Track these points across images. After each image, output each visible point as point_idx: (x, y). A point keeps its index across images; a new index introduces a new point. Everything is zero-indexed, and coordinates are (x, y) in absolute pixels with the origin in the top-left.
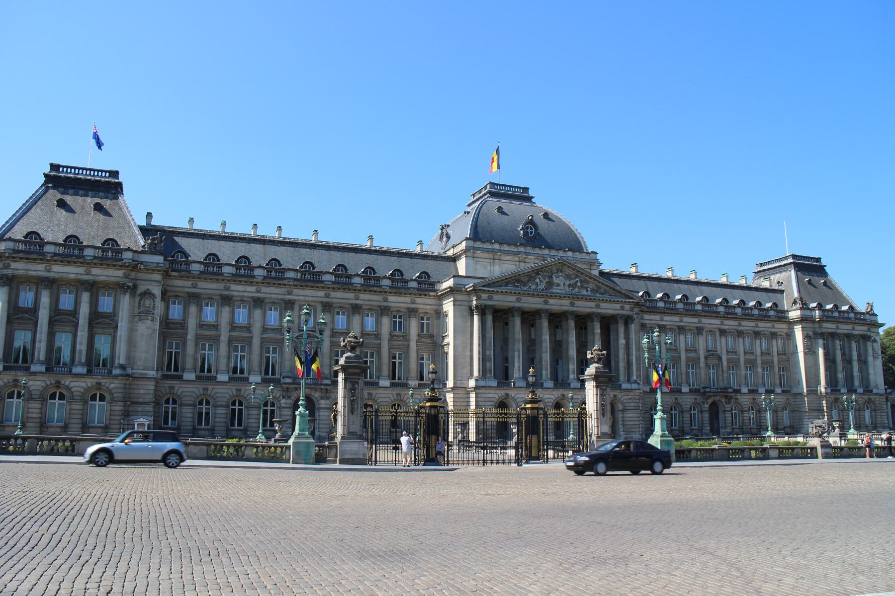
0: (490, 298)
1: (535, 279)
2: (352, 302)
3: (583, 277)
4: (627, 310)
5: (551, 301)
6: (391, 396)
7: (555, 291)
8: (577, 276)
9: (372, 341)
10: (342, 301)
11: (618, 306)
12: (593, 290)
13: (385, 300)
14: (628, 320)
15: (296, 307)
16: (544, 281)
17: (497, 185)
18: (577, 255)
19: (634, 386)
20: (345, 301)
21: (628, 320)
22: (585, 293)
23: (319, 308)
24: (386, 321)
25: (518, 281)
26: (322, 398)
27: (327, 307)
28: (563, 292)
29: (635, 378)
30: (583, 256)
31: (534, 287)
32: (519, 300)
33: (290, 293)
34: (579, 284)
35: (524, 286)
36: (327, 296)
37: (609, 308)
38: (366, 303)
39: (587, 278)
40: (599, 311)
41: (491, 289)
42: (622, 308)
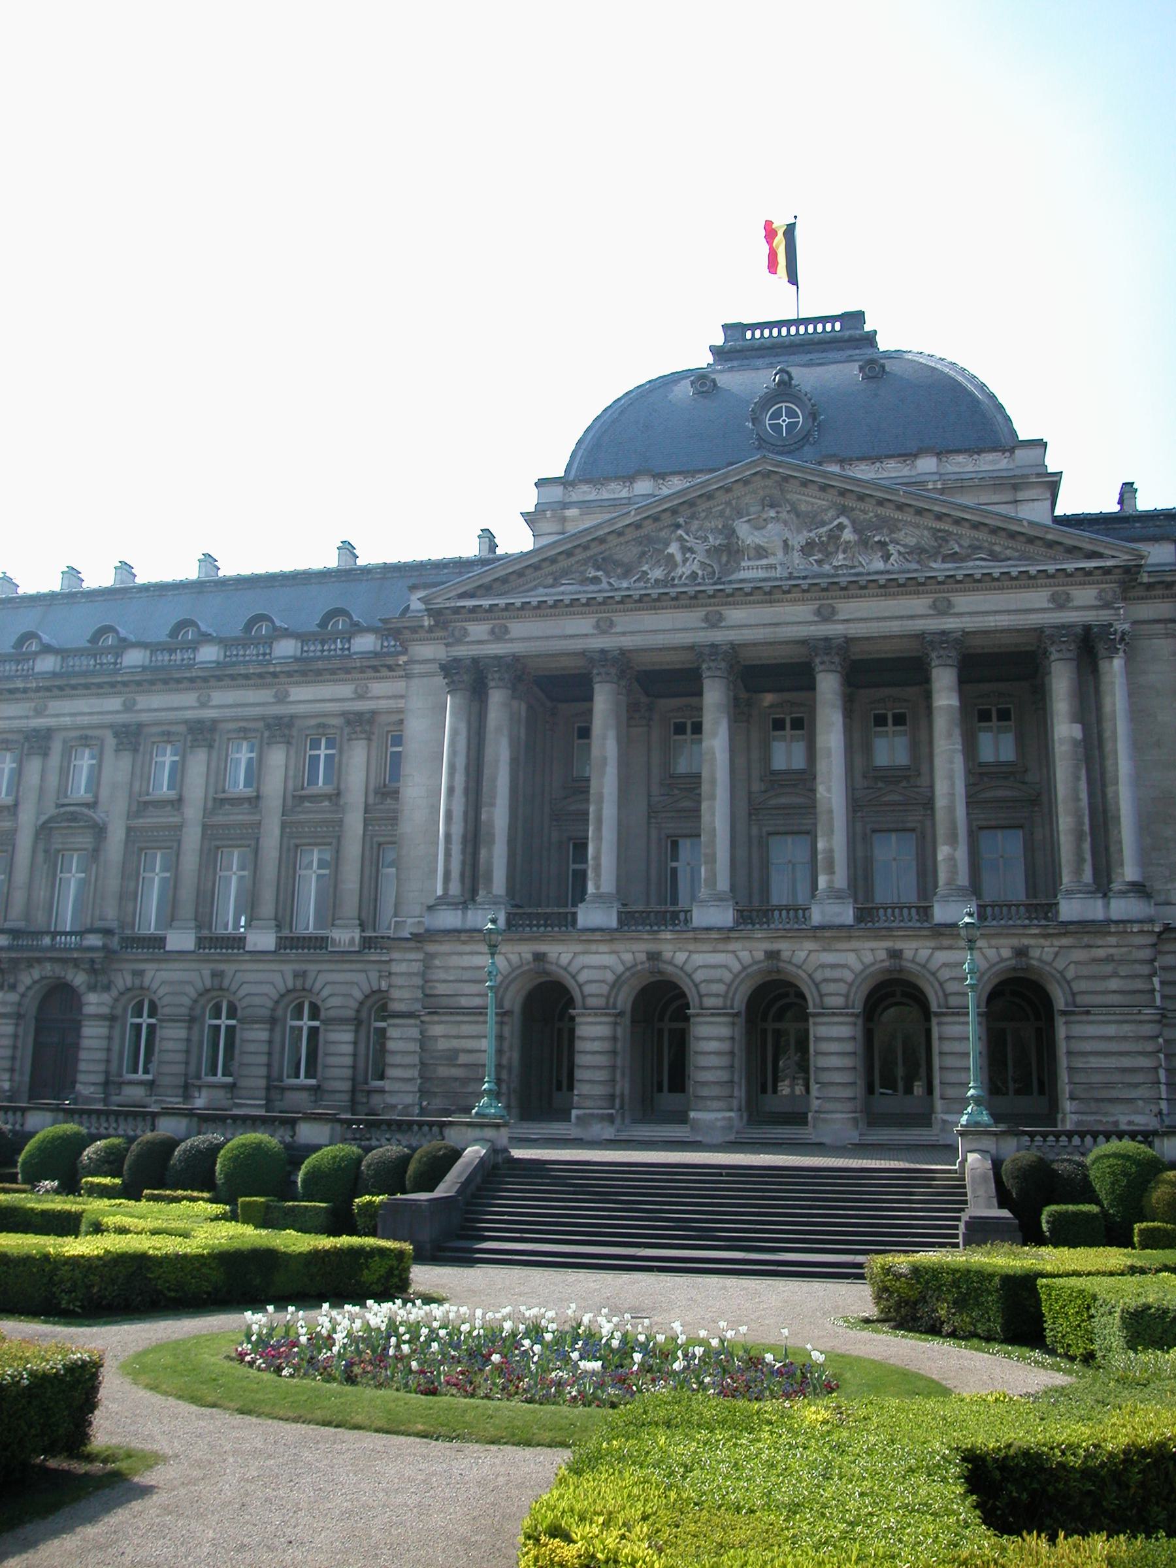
0: (499, 634)
1: (667, 545)
2: (190, 714)
3: (870, 512)
4: (1084, 605)
5: (735, 615)
6: (277, 978)
7: (743, 575)
8: (843, 510)
9: (239, 816)
10: (163, 715)
11: (1038, 598)
12: (918, 552)
13: (281, 699)
14: (1089, 647)
15: (57, 747)
16: (700, 548)
17: (753, 327)
18: (960, 464)
19: (1122, 908)
20: (171, 715)
21: (1089, 647)
22: (879, 565)
23: (111, 742)
24: (277, 757)
25: (605, 563)
26: (92, 988)
27: (131, 737)
28: (779, 572)
29: (1130, 872)
30: (991, 463)
31: (657, 573)
32: (604, 628)
33: (39, 713)
34: (848, 535)
35: (626, 575)
36: (128, 707)
37: (993, 613)
38: (228, 712)
39: (888, 512)
40: (950, 624)
41: (486, 603)
42: (1061, 602)
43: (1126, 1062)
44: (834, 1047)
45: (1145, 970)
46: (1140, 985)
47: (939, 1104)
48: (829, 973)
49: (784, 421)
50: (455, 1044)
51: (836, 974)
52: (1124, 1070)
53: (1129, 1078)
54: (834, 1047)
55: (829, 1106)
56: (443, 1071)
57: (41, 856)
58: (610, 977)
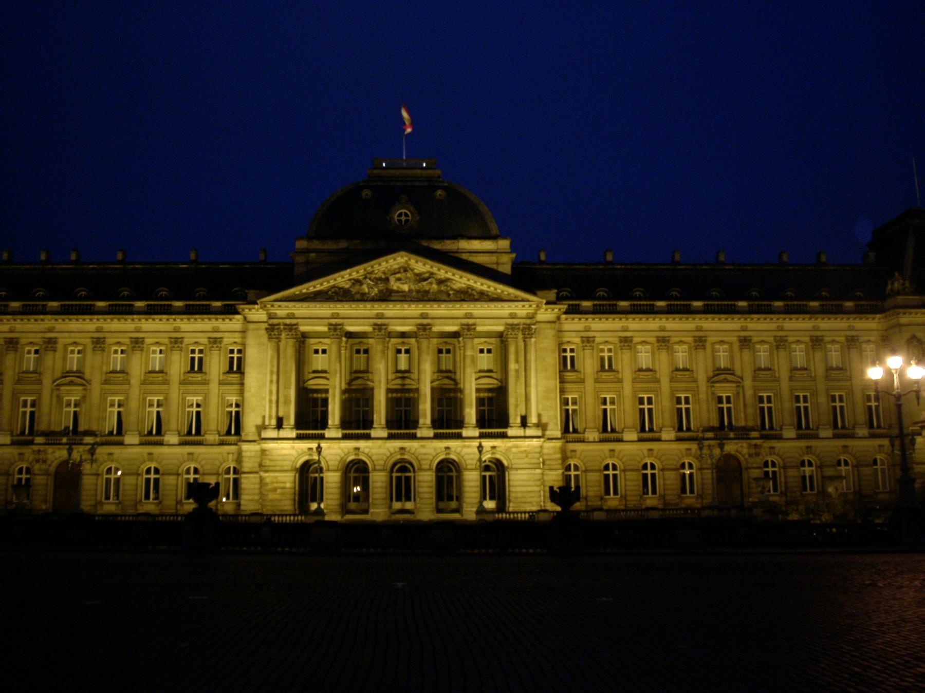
43: (530, 489)
44: (425, 484)
45: (537, 455)
46: (536, 461)
47: (465, 505)
48: (423, 457)
49: (403, 218)
50: (275, 485)
51: (427, 457)
52: (529, 492)
53: (530, 495)
54: (425, 484)
55: (423, 506)
56: (271, 496)
57: (55, 399)
58: (339, 458)
